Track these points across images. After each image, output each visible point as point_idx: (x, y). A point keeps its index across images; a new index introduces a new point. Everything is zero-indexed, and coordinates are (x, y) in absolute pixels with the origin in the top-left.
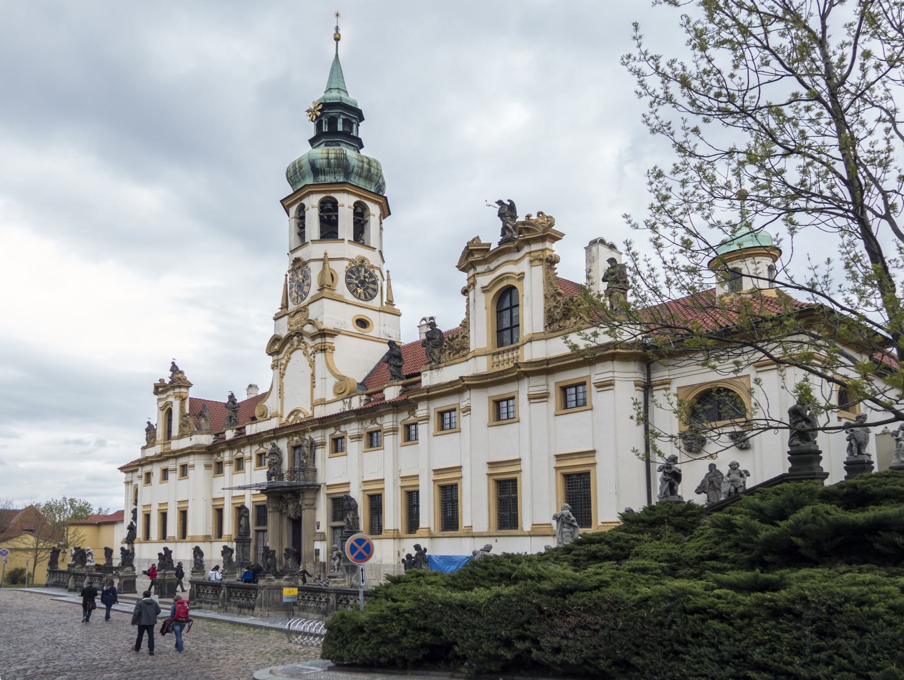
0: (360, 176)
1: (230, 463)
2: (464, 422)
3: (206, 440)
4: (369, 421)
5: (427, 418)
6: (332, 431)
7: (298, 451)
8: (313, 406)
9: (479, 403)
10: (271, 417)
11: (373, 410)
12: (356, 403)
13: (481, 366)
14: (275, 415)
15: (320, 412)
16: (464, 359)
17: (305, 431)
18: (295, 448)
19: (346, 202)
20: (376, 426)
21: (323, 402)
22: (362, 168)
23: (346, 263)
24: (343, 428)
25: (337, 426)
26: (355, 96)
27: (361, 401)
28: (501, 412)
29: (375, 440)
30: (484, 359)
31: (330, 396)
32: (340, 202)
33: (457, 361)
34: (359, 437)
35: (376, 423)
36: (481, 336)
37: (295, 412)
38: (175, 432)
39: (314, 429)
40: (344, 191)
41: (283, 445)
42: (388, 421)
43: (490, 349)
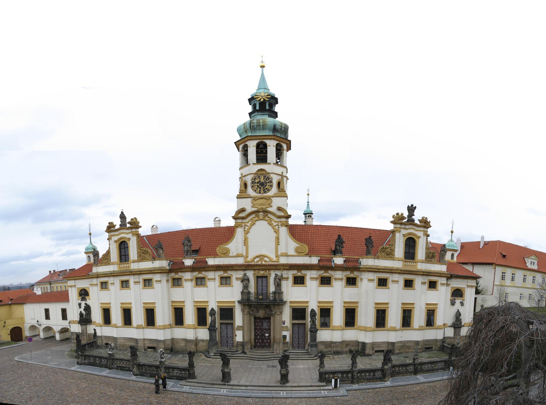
6: (295, 272)
7: (260, 280)
8: (277, 256)
11: (325, 266)
12: (314, 260)
14: (238, 256)
15: (283, 261)
20: (327, 274)
21: (287, 255)
24: (304, 272)
31: (292, 252)
34: (317, 279)
37: (261, 257)
39: (284, 269)
41: (250, 274)
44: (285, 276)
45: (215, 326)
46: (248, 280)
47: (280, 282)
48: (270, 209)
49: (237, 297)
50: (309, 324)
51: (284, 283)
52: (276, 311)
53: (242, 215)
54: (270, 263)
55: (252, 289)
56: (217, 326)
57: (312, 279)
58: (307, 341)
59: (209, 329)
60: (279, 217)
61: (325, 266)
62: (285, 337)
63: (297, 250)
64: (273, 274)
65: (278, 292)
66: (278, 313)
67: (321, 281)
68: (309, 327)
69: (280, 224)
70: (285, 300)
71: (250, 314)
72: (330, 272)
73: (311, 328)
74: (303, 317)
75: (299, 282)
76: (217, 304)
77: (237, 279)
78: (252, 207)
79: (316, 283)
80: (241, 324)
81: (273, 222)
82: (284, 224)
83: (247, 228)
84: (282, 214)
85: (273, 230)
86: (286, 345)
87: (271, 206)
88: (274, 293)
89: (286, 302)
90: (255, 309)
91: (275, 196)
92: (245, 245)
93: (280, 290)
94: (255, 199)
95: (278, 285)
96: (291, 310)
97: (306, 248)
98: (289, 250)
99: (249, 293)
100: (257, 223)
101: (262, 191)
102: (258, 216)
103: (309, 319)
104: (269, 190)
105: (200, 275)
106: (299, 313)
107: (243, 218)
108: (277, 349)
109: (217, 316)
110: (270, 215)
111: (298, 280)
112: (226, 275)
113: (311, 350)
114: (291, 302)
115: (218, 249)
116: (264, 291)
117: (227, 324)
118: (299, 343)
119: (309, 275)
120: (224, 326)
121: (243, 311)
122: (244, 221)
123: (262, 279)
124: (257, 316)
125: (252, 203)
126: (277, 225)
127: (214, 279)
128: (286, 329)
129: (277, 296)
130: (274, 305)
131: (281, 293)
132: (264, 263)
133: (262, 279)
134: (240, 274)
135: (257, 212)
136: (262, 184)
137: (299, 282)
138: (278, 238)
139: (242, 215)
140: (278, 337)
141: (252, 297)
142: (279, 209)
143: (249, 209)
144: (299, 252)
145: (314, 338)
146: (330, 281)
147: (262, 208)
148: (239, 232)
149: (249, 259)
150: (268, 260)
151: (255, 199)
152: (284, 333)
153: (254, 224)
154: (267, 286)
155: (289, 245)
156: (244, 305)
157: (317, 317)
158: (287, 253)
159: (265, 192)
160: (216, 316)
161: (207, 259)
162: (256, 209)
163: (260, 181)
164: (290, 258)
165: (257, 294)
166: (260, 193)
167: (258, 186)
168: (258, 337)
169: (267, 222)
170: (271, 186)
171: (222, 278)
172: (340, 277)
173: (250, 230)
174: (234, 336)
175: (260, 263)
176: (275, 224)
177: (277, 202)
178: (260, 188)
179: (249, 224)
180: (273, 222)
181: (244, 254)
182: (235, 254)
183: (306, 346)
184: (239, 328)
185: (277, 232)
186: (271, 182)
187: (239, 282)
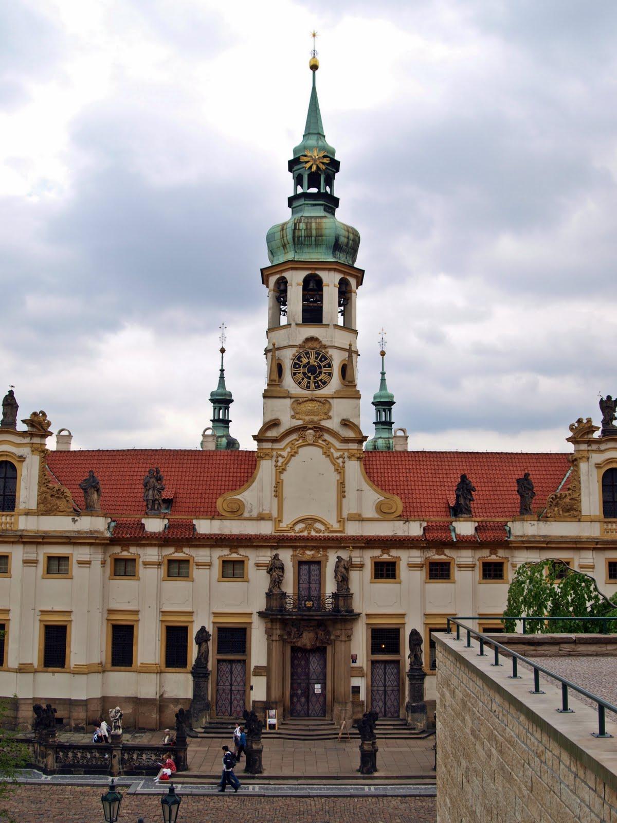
1: (159, 564)
3: (98, 524)
4: (434, 551)
6: (377, 553)
7: (305, 568)
8: (341, 521)
11: (437, 540)
12: (415, 529)
14: (261, 518)
15: (353, 530)
20: (443, 557)
24: (394, 553)
31: (370, 512)
34: (421, 566)
37: (310, 521)
39: (354, 548)
41: (286, 556)
44: (356, 561)
45: (206, 667)
46: (282, 568)
47: (348, 572)
48: (326, 424)
49: (259, 603)
50: (408, 661)
51: (354, 575)
52: (338, 633)
53: (272, 433)
54: (326, 534)
55: (289, 588)
56: (210, 667)
57: (411, 566)
58: (404, 698)
59: (192, 673)
60: (346, 441)
61: (437, 540)
62: (356, 690)
63: (379, 508)
64: (332, 558)
65: (343, 593)
66: (343, 638)
67: (431, 570)
68: (408, 668)
69: (346, 454)
70: (356, 611)
71: (284, 641)
72: (447, 552)
73: (412, 669)
74: (395, 648)
75: (385, 572)
76: (212, 619)
77: (258, 565)
78: (293, 417)
79: (419, 576)
80: (263, 662)
81: (332, 450)
82: (354, 455)
83: (281, 460)
84: (350, 434)
85: (332, 468)
86: (359, 709)
87: (330, 418)
88: (335, 596)
89: (359, 614)
90: (294, 630)
91: (338, 396)
92: (276, 496)
93: (348, 589)
94: (298, 401)
95: (343, 580)
96: (370, 631)
97: (398, 504)
98: (364, 508)
99: (284, 595)
100: (301, 450)
101: (312, 385)
102: (304, 438)
103: (408, 652)
104: (325, 383)
105: (179, 555)
106: (385, 639)
107: (274, 440)
108: (339, 718)
109: (212, 646)
110: (327, 436)
111: (382, 570)
112: (234, 556)
113: (413, 719)
114: (368, 616)
115: (220, 501)
116: (314, 593)
117: (231, 662)
118: (385, 704)
119: (405, 558)
120: (225, 667)
121: (269, 633)
122: (276, 446)
123: (309, 569)
124: (299, 644)
125: (293, 409)
126: (341, 457)
127: (209, 565)
128: (360, 673)
129: (341, 603)
130: (335, 621)
131: (348, 596)
132: (313, 533)
133: (309, 569)
134: (265, 556)
135: (303, 428)
136: (313, 370)
137: (385, 572)
138: (342, 484)
139: (272, 433)
140: (342, 689)
141: (289, 605)
142: (346, 423)
143: (287, 422)
144: (384, 513)
145: (418, 692)
146: (448, 570)
147: (312, 422)
148: (266, 469)
149: (283, 526)
150: (322, 528)
151: (298, 401)
152: (356, 682)
153: (296, 453)
154: (320, 581)
155: (366, 497)
156: (272, 621)
157: (423, 646)
158: (360, 515)
159: (318, 387)
160: (210, 643)
161: (195, 522)
162: (300, 423)
163: (308, 363)
164: (365, 524)
165: (299, 598)
166: (308, 387)
167: (304, 374)
168: (299, 692)
169: (318, 451)
170: (330, 374)
171: (225, 563)
172: (469, 561)
174: (248, 688)
175: (305, 534)
176: (336, 454)
177: (340, 409)
178: (310, 378)
180: (332, 450)
181: (275, 514)
182: (255, 514)
183: (402, 712)
184: (259, 671)
185: (340, 470)
186: (330, 365)
187: (263, 572)
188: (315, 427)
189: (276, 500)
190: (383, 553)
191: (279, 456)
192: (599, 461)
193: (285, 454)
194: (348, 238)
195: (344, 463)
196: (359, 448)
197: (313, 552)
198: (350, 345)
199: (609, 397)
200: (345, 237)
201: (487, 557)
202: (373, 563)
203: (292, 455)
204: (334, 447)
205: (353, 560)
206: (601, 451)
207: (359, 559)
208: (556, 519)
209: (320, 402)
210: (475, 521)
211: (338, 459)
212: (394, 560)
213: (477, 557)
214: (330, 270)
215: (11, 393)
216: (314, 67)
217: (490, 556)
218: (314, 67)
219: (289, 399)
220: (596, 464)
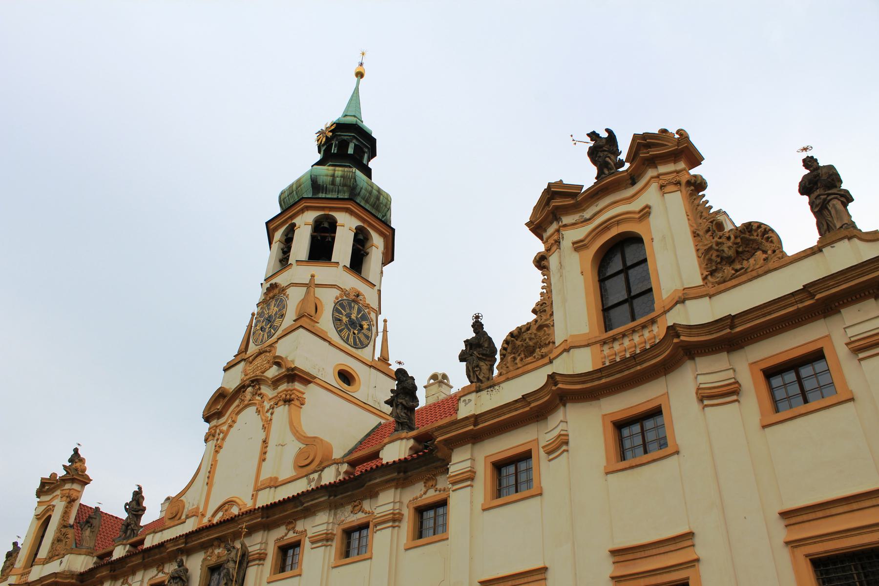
0: (367, 201)
2: (548, 472)
4: (349, 508)
5: (469, 477)
9: (586, 428)
10: (187, 517)
13: (581, 362)
16: (546, 360)
17: (237, 535)
18: (214, 570)
19: (346, 227)
20: (361, 515)
21: (274, 484)
22: (370, 193)
23: (337, 293)
24: (300, 526)
25: (289, 521)
26: (369, 123)
27: (338, 473)
28: (638, 437)
29: (355, 544)
30: (587, 351)
31: (287, 471)
32: (339, 222)
33: (530, 367)
34: (326, 539)
35: (361, 510)
36: (577, 315)
38: (43, 553)
39: (252, 530)
40: (347, 210)
42: (385, 502)
43: (597, 334)
81: (265, 403)
104: (276, 330)
138: (265, 442)
149: (205, 521)
153: (234, 422)
158: (276, 478)
164: (279, 489)
170: (282, 316)
173: (226, 445)
176: (267, 405)
179: (225, 428)
188: (252, 381)
189: (206, 488)
190: (289, 530)
191: (221, 432)
192: (581, 237)
193: (225, 428)
194: (333, 176)
195: (272, 414)
196: (290, 388)
197: (220, 551)
198: (313, 276)
199: (593, 135)
200: (327, 176)
201: (421, 497)
202: (276, 548)
203: (231, 426)
204: (267, 396)
205: (250, 549)
206: (589, 219)
207: (258, 547)
208: (510, 375)
209: (266, 351)
210: (408, 439)
211: (267, 411)
212: (297, 539)
213: (406, 501)
214: (302, 211)
215: (76, 451)
216: (360, 75)
217: (425, 493)
218: (360, 75)
219: (243, 364)
220: (574, 243)
